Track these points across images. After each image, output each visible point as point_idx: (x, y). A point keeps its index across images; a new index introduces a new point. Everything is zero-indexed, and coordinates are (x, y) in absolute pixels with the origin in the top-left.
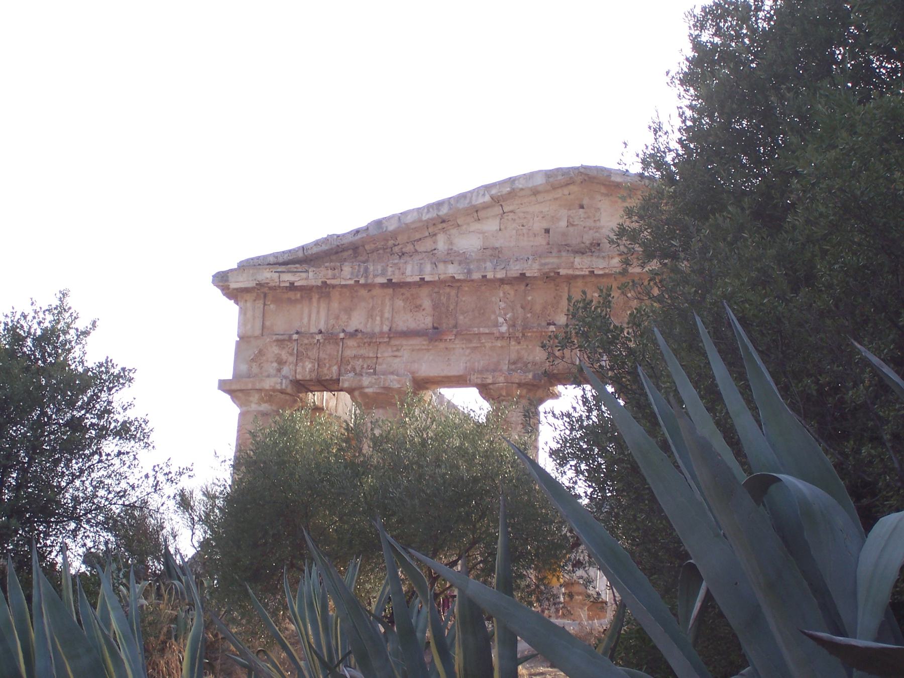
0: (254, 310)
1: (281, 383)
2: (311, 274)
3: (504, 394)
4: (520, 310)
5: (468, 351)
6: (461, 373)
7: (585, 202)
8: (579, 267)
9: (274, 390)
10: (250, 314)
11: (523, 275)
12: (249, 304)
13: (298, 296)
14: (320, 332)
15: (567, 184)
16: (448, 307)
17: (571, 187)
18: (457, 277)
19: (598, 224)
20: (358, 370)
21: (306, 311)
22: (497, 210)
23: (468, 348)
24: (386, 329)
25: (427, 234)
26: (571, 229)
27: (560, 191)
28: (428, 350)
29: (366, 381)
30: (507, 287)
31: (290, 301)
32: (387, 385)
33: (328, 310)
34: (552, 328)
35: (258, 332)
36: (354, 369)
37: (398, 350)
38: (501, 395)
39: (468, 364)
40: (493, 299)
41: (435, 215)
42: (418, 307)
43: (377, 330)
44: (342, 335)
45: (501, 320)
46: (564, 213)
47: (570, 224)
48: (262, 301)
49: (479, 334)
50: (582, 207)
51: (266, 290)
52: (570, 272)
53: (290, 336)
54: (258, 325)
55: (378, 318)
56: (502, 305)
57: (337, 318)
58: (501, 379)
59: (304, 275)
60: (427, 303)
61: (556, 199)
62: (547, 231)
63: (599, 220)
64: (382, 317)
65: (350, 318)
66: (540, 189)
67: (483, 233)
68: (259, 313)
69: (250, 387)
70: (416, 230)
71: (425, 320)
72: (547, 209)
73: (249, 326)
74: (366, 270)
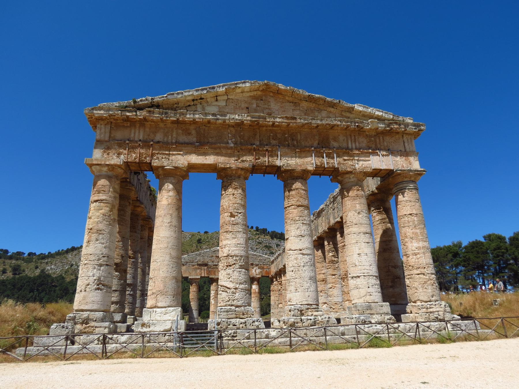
0: (105, 128)
1: (120, 162)
2: (138, 113)
4: (238, 138)
6: (212, 163)
7: (264, 98)
9: (116, 165)
10: (103, 130)
12: (102, 126)
13: (129, 125)
14: (140, 140)
16: (204, 134)
20: (160, 158)
21: (133, 131)
22: (225, 97)
24: (174, 141)
26: (258, 108)
27: (253, 92)
29: (165, 164)
30: (232, 129)
31: (124, 126)
32: (176, 166)
33: (144, 132)
34: (254, 146)
35: (107, 139)
36: (158, 158)
38: (232, 173)
42: (190, 134)
43: (170, 141)
44: (152, 143)
45: (230, 141)
46: (254, 101)
47: (257, 106)
48: (109, 125)
50: (262, 100)
51: (112, 120)
53: (125, 142)
54: (107, 135)
55: (170, 137)
56: (230, 135)
57: (149, 135)
59: (134, 113)
60: (194, 132)
62: (247, 108)
64: (172, 136)
65: (155, 136)
66: (245, 90)
67: (219, 106)
68: (108, 130)
69: (103, 163)
70: (188, 101)
71: (193, 138)
73: (102, 136)
74: (166, 113)
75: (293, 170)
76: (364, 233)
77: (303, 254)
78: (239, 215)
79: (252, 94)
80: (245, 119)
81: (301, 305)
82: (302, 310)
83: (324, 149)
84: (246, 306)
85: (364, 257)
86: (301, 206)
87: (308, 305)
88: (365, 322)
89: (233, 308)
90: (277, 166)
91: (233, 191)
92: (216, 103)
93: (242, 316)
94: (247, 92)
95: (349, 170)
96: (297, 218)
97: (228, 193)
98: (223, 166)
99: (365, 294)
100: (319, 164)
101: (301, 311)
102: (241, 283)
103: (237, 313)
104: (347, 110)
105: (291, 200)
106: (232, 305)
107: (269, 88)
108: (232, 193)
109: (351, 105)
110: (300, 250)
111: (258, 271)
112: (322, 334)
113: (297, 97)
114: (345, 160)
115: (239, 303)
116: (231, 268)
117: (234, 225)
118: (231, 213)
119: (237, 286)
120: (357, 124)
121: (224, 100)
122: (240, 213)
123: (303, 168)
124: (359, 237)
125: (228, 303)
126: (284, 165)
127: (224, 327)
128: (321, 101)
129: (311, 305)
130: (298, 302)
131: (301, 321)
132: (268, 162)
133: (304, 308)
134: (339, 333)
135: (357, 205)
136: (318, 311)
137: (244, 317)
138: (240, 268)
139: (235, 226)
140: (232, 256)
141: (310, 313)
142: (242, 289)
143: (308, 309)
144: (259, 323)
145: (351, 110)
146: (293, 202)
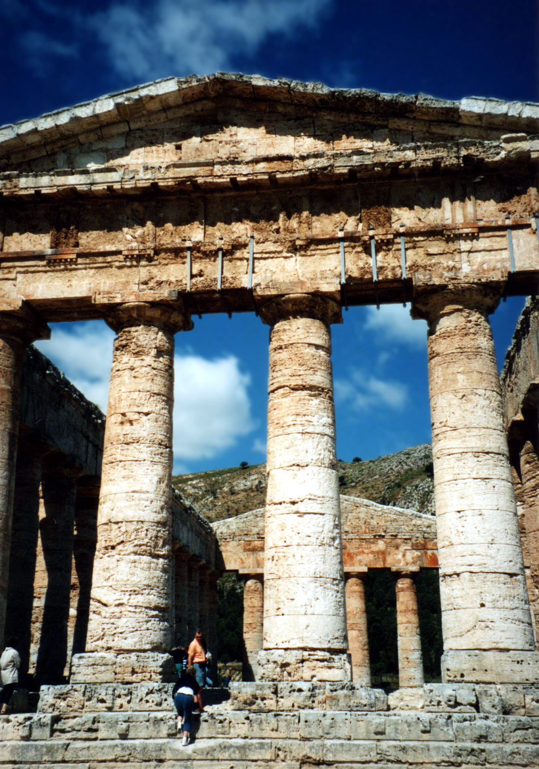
3: (135, 315)
5: (93, 271)
8: (219, 174)
11: (154, 185)
15: (200, 99)
17: (205, 102)
18: (79, 188)
19: (234, 138)
23: (92, 268)
25: (44, 153)
28: (46, 272)
30: (136, 205)
37: (10, 272)
39: (92, 286)
40: (120, 217)
41: (53, 125)
49: (105, 254)
52: (209, 180)
58: (132, 298)
61: (187, 116)
63: (236, 134)
70: (32, 147)
72: (178, 126)
75: (283, 295)
76: (477, 454)
77: (300, 514)
78: (145, 418)
79: (190, 110)
80: (160, 176)
81: (286, 649)
82: (287, 665)
83: (371, 233)
84: (145, 651)
85: (472, 520)
86: (304, 388)
87: (304, 649)
88: (457, 704)
89: (110, 656)
90: (243, 289)
91: (133, 359)
92: (102, 145)
93: (128, 677)
94: (178, 106)
95: (437, 281)
96: (289, 420)
97: (120, 367)
98: (105, 301)
99: (471, 624)
100: (356, 274)
101: (284, 665)
102: (135, 592)
103: (118, 670)
104: (443, 118)
105: (279, 374)
106: (109, 648)
107: (231, 88)
108: (129, 366)
109: (448, 104)
110: (293, 503)
111: (411, 555)
112: (320, 733)
113: (304, 102)
114: (429, 255)
115: (126, 645)
116: (114, 552)
117: (127, 444)
118: (124, 415)
119: (125, 601)
120: (464, 153)
121: (119, 135)
122: (147, 414)
123: (310, 287)
124: (461, 463)
125: (100, 643)
126: (259, 285)
127: (77, 706)
128: (368, 104)
129: (314, 650)
130: (279, 642)
131: (275, 692)
132: (222, 282)
133: (291, 657)
134: (368, 732)
135: (460, 377)
136: (330, 668)
137: (134, 678)
138: (136, 553)
139: (130, 447)
140: (117, 523)
141: (307, 674)
142: (136, 607)
143: (303, 661)
144: (164, 696)
145: (452, 117)
146: (281, 379)
